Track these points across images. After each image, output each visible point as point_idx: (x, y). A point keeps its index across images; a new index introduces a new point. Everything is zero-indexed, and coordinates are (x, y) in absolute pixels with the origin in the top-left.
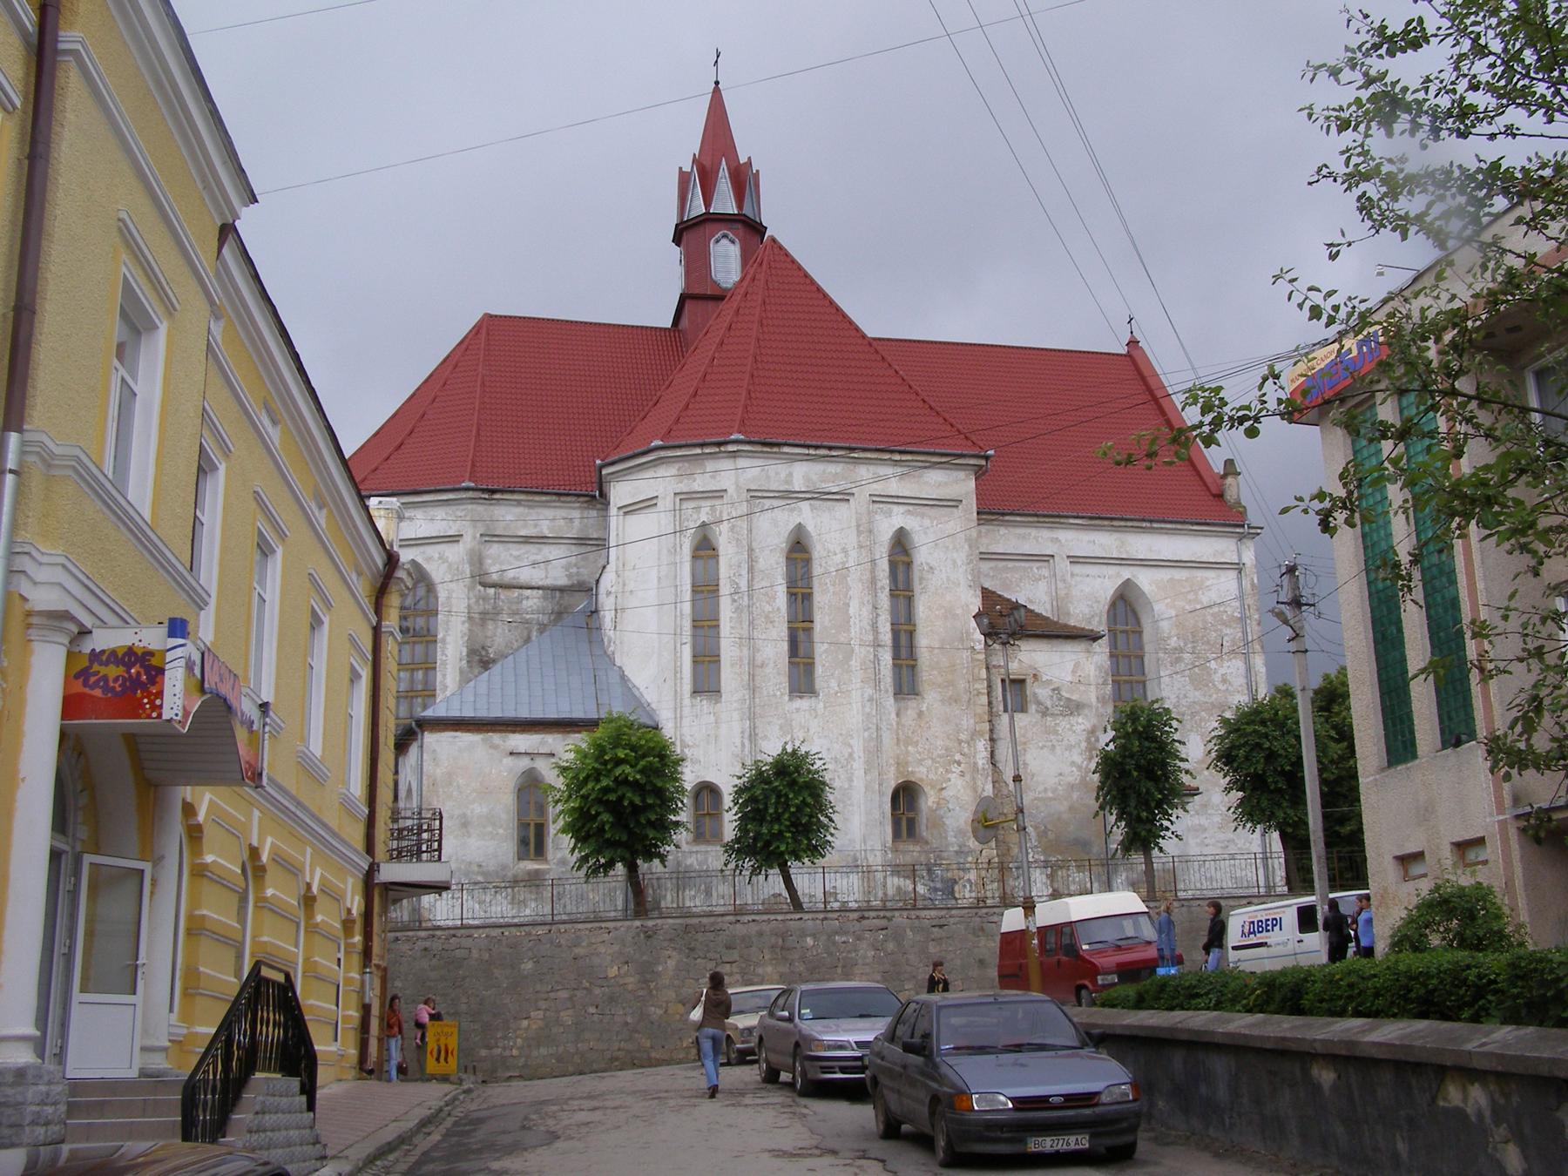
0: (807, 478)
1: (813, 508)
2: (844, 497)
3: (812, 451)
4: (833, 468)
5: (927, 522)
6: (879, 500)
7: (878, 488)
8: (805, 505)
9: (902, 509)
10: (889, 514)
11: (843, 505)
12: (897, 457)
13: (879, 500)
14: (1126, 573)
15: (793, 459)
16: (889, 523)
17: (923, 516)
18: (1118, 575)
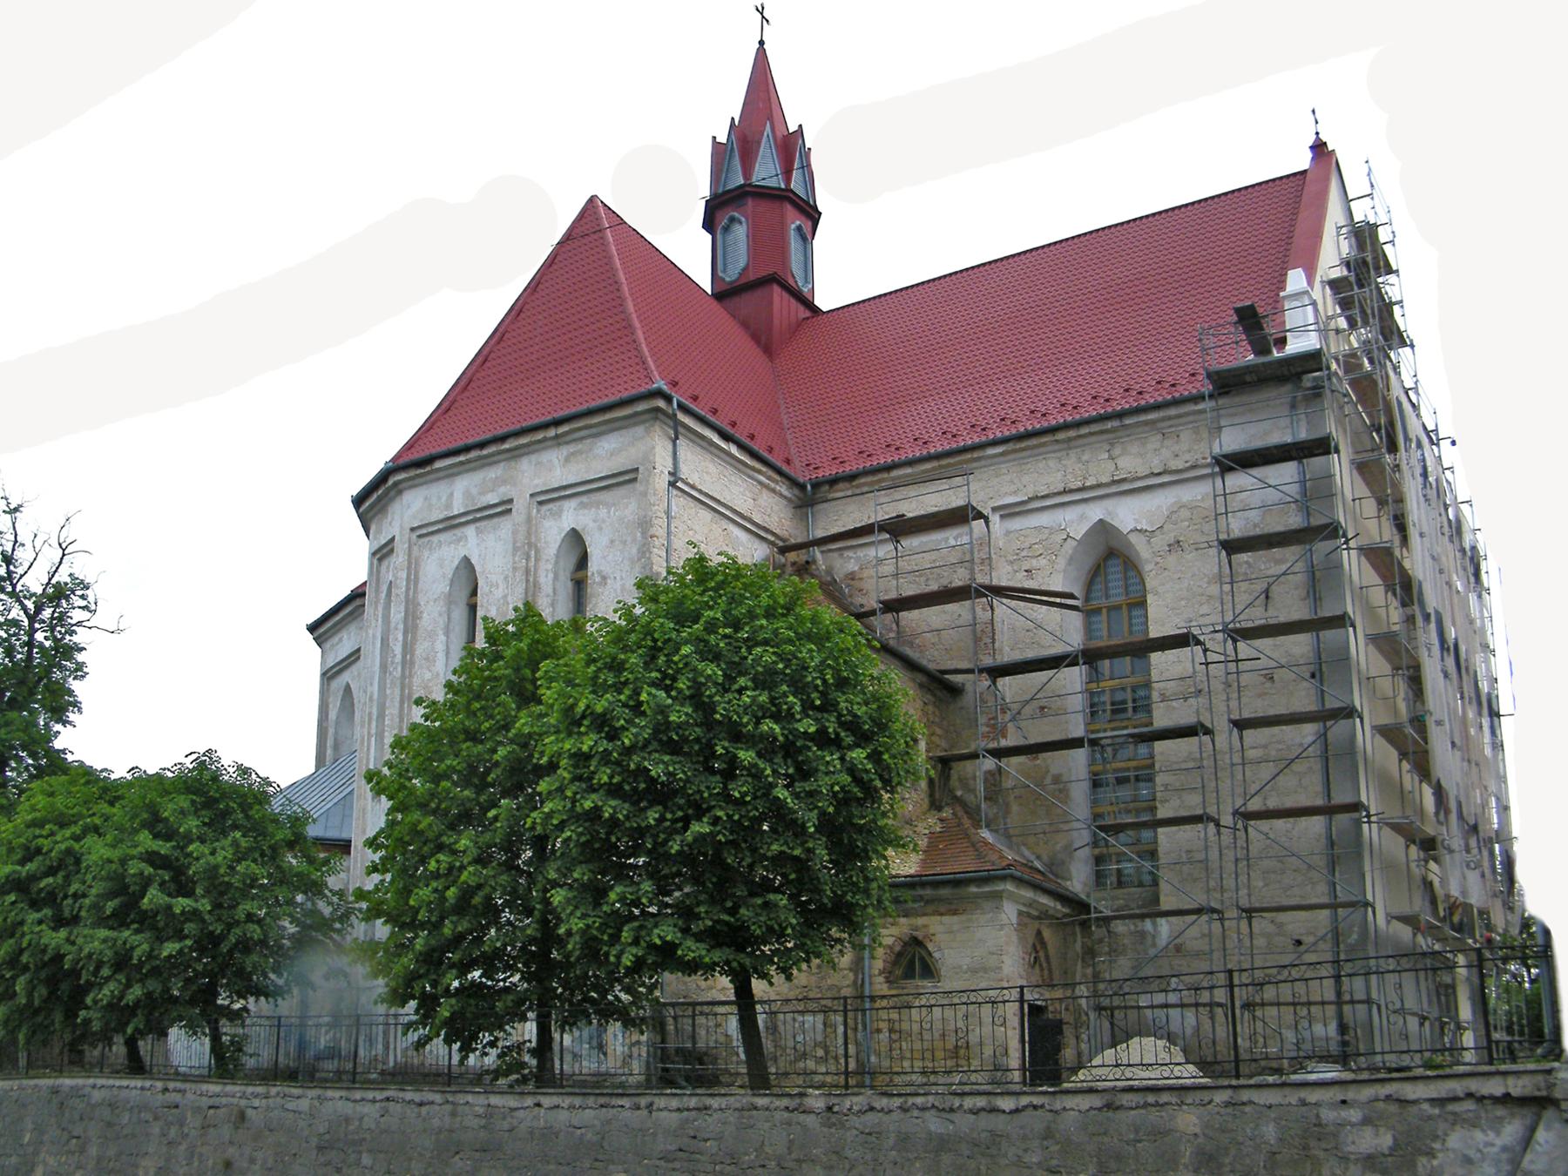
0: (467, 494)
1: (479, 531)
2: (504, 508)
3: (462, 458)
4: (493, 473)
5: (603, 512)
6: (549, 498)
7: (540, 483)
8: (470, 531)
9: (573, 503)
10: (559, 514)
11: (507, 517)
12: (552, 432)
13: (549, 498)
14: (1095, 512)
15: (451, 474)
16: (553, 531)
17: (597, 505)
18: (1082, 517)
